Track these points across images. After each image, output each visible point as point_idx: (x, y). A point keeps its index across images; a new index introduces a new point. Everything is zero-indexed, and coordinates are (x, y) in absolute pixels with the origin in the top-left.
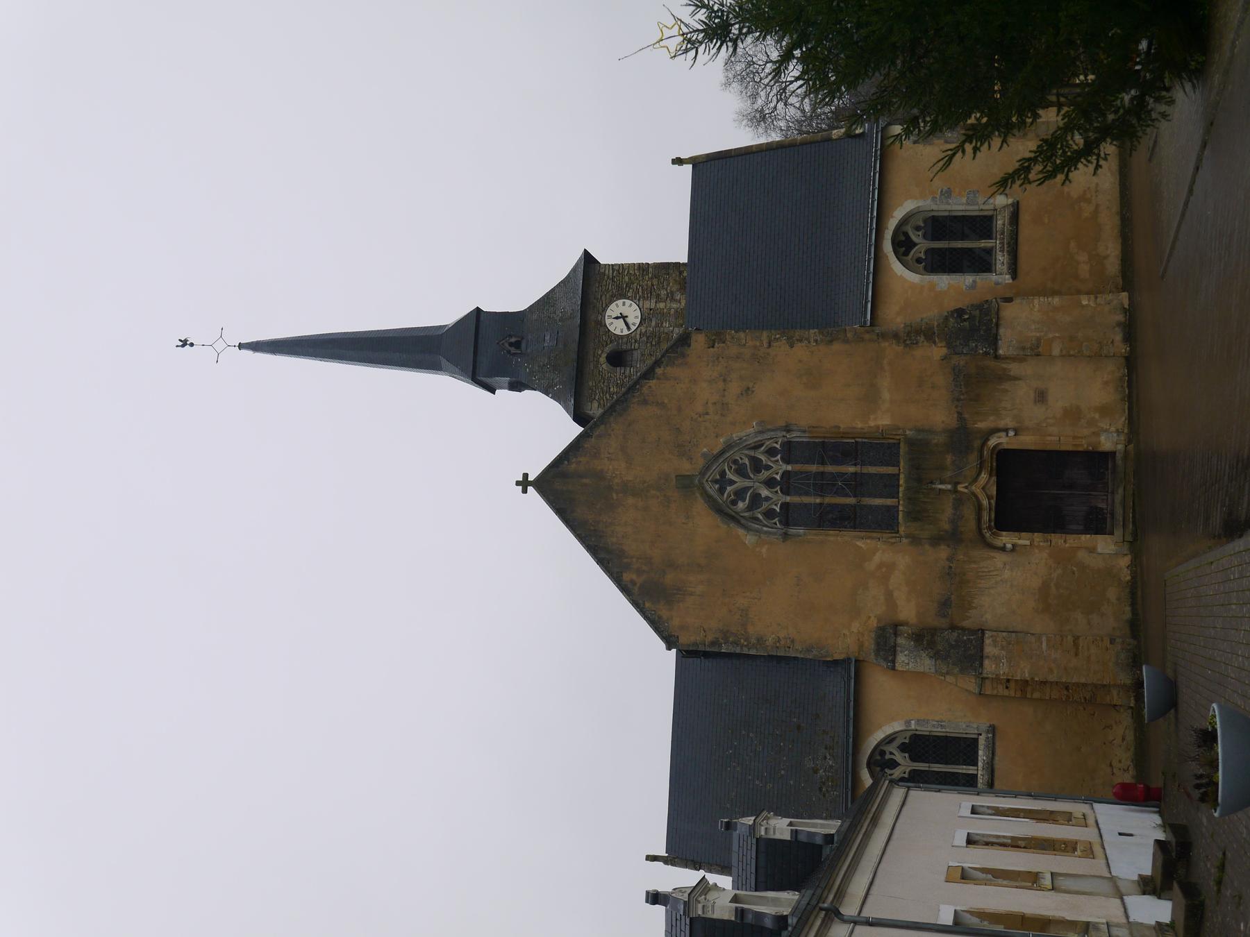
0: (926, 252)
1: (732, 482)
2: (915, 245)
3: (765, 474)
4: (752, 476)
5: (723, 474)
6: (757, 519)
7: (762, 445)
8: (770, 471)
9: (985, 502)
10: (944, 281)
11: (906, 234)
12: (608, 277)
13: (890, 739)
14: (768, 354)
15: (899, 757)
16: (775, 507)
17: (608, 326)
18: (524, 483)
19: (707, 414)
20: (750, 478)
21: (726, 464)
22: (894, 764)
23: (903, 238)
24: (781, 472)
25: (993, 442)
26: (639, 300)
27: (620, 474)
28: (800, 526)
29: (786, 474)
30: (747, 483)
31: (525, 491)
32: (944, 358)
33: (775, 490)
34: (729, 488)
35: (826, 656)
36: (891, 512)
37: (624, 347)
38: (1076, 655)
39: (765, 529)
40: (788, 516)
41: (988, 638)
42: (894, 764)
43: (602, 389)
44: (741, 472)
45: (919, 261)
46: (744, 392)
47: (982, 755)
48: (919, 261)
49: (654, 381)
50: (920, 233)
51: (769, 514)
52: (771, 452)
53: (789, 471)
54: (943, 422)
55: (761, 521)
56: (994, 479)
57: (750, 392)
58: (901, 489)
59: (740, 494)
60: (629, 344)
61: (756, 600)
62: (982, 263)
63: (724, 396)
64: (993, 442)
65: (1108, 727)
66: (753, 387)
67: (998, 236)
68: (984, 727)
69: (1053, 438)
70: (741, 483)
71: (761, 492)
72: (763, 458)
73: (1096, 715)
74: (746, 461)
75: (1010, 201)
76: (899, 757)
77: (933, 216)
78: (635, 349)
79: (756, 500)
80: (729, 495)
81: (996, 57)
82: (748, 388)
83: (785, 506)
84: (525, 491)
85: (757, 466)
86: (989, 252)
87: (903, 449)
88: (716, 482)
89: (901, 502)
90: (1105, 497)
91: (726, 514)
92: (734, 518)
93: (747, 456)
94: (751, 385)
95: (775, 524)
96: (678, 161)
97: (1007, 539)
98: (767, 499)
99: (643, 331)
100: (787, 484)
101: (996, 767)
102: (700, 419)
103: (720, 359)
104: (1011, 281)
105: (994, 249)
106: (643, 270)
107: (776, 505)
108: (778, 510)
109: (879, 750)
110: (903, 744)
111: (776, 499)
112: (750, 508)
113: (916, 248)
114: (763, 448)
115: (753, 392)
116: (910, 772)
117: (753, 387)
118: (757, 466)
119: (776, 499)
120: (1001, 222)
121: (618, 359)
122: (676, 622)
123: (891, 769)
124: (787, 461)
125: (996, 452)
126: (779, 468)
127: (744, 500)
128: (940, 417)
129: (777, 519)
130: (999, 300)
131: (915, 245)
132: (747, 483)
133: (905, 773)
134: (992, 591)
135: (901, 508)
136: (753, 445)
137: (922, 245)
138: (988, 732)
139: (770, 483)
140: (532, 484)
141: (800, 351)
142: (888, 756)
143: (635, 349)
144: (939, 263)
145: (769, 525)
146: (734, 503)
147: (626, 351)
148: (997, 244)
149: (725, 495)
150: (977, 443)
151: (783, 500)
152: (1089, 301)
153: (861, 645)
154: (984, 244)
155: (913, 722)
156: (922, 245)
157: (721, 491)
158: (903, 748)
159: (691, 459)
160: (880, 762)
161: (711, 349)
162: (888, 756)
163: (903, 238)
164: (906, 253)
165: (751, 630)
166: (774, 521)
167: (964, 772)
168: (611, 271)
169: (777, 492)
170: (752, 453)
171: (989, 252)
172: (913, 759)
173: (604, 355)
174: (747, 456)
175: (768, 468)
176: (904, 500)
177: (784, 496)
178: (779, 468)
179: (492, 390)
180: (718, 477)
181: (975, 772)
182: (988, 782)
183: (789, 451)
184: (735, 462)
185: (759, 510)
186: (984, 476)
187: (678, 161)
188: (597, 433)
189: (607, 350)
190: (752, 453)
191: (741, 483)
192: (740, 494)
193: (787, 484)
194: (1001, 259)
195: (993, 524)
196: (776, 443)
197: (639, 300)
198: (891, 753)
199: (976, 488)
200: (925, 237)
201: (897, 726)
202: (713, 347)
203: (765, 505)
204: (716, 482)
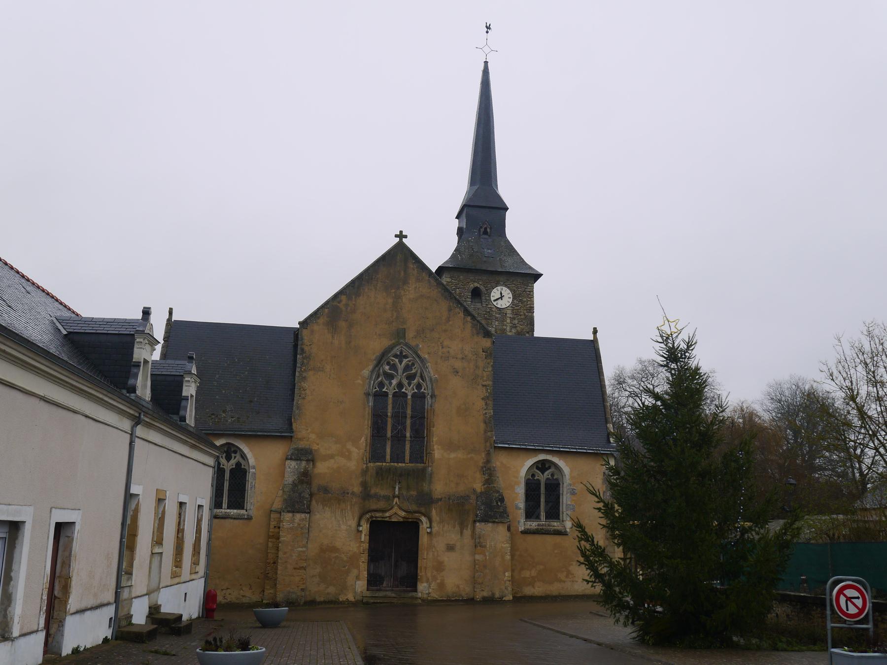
0: (538, 480)
1: (401, 362)
2: (543, 473)
3: (405, 382)
4: (404, 374)
5: (406, 357)
6: (378, 377)
7: (423, 381)
9: (387, 514)
10: (521, 490)
11: (549, 468)
12: (526, 288)
13: (243, 456)
14: (478, 385)
15: (233, 462)
16: (385, 388)
17: (496, 288)
18: (401, 236)
19: (442, 348)
20: (403, 373)
22: (228, 459)
23: (547, 466)
24: (407, 392)
25: (423, 519)
26: (512, 307)
29: (405, 395)
30: (400, 371)
31: (396, 236)
32: (474, 490)
33: (396, 389)
34: (397, 360)
36: (382, 458)
37: (483, 298)
39: (372, 382)
40: (380, 396)
41: (305, 516)
42: (228, 459)
43: (458, 284)
44: (407, 368)
45: (533, 475)
46: (455, 370)
48: (533, 475)
49: (463, 316)
50: (550, 476)
51: (381, 385)
52: (419, 386)
53: (407, 397)
54: (436, 490)
55: (377, 380)
56: (402, 520)
57: (455, 374)
58: (396, 464)
60: (485, 301)
62: (531, 513)
64: (423, 519)
65: (251, 587)
66: (458, 376)
67: (547, 523)
68: (251, 513)
70: (401, 367)
71: (395, 380)
74: (413, 371)
75: (568, 530)
76: (233, 462)
77: (560, 484)
78: (482, 304)
79: (390, 377)
82: (458, 373)
84: (396, 236)
86: (538, 517)
87: (420, 465)
88: (401, 352)
89: (388, 464)
90: (389, 586)
92: (379, 363)
93: (417, 371)
94: (460, 374)
96: (595, 331)
97: (365, 527)
98: (391, 384)
99: (493, 310)
100: (399, 395)
101: (227, 520)
102: (439, 343)
103: (476, 356)
104: (520, 530)
105: (539, 520)
106: (529, 310)
108: (384, 390)
109: (237, 450)
110: (241, 465)
111: (390, 388)
112: (385, 374)
113: (541, 474)
114: (421, 381)
115: (456, 376)
118: (411, 378)
119: (390, 388)
120: (555, 525)
121: (476, 294)
122: (316, 327)
124: (413, 396)
125: (417, 521)
126: (409, 391)
127: (390, 369)
128: (439, 487)
130: (509, 523)
131: (543, 473)
132: (400, 371)
133: (223, 465)
134: (333, 518)
135: (384, 464)
136: (423, 375)
137: (543, 477)
139: (400, 385)
141: (480, 404)
143: (482, 304)
144: (532, 488)
146: (388, 364)
147: (481, 299)
148: (543, 522)
149: (393, 358)
150: (423, 510)
151: (389, 393)
152: (507, 577)
153: (301, 439)
154: (543, 515)
155: (254, 470)
156: (543, 477)
157: (396, 356)
158: (238, 464)
159: (415, 338)
160: (229, 451)
161: (482, 351)
162: (233, 455)
163: (547, 466)
164: (538, 468)
165: (311, 373)
167: (224, 501)
168: (529, 290)
169: (395, 389)
170: (418, 374)
171: (538, 517)
172: (232, 471)
173: (478, 286)
174: (417, 371)
175: (409, 384)
178: (409, 391)
179: (457, 217)
180: (404, 354)
183: (419, 397)
184: (413, 364)
185: (384, 379)
186: (403, 514)
187: (595, 331)
189: (482, 288)
190: (418, 374)
191: (401, 367)
192: (393, 367)
193: (399, 395)
194: (533, 525)
195: (374, 519)
196: (424, 389)
197: (512, 307)
198: (235, 457)
199: (395, 509)
200: (547, 479)
201: (252, 461)
202: (483, 352)
203: (387, 382)
204: (401, 352)
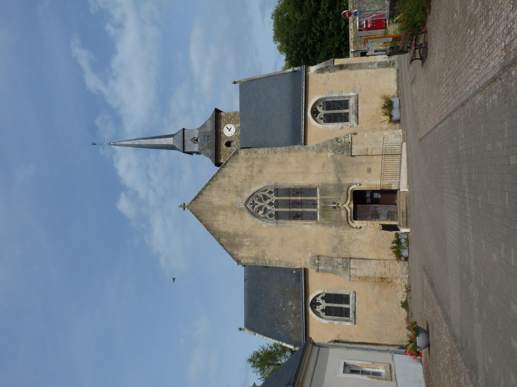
0: (324, 115)
1: (257, 204)
2: (320, 112)
3: (268, 201)
4: (264, 202)
5: (253, 201)
6: (267, 217)
7: (267, 190)
8: (271, 200)
9: (349, 210)
10: (331, 126)
11: (316, 109)
12: (224, 117)
13: (318, 296)
14: (267, 157)
15: (321, 301)
16: (273, 213)
17: (225, 133)
18: (184, 206)
19: (246, 180)
20: (263, 202)
21: (254, 198)
22: (319, 304)
23: (315, 110)
24: (274, 200)
25: (351, 189)
26: (234, 124)
27: (217, 203)
28: (282, 219)
29: (276, 201)
30: (262, 204)
31: (184, 209)
32: (332, 156)
33: (273, 207)
34: (256, 206)
35: (294, 267)
36: (315, 214)
37: (230, 140)
38: (385, 267)
39: (270, 221)
40: (278, 216)
41: (352, 262)
42: (319, 304)
43: (224, 155)
44: (260, 200)
45: (321, 119)
46: (259, 172)
47: (351, 301)
48: (321, 119)
49: (227, 168)
50: (321, 108)
51: (271, 215)
52: (270, 192)
53: (277, 200)
54: (332, 181)
55: (268, 218)
56: (352, 201)
57: (261, 171)
58: (318, 206)
59: (260, 208)
60: (232, 139)
61: (267, 247)
62: (344, 118)
63: (252, 173)
64: (351, 189)
65: (397, 291)
66: (262, 169)
67: (351, 108)
68: (351, 292)
69: (374, 186)
70: (260, 204)
71: (267, 207)
72: (268, 195)
73: (393, 287)
74: (261, 196)
75: (355, 94)
76: (321, 301)
77: (326, 101)
78: (234, 141)
79: (266, 210)
80: (256, 209)
81: (275, 322)
82: (261, 170)
83: (276, 212)
84: (184, 209)
85: (265, 198)
86: (347, 114)
87: (318, 191)
88: (251, 204)
89: (318, 210)
90: (394, 207)
91: (254, 215)
92: (258, 217)
93: (261, 194)
94: (261, 168)
95: (273, 219)
96: (235, 83)
97: (357, 223)
98: (270, 210)
99: (236, 134)
100: (277, 204)
101: (357, 306)
102: (244, 182)
103: (250, 159)
104: (356, 126)
105: (349, 113)
106: (235, 114)
107: (273, 212)
108: (274, 214)
109: (314, 299)
110: (323, 297)
111: (273, 210)
112: (264, 213)
113: (320, 113)
114: (267, 192)
115: (262, 171)
116: (326, 307)
117: (262, 169)
118: (265, 198)
119: (273, 210)
120: (352, 102)
121: (228, 144)
122: (240, 255)
123: (319, 306)
124: (276, 195)
125: (353, 191)
126: (273, 198)
127: (261, 210)
128: (331, 179)
129: (274, 217)
130: (352, 134)
131: (320, 112)
132: (262, 204)
133: (324, 307)
134: (353, 243)
135: (318, 213)
136: (264, 190)
137: (322, 112)
138: (353, 293)
139: (270, 204)
140: (188, 207)
141: (278, 155)
142: (317, 301)
143: (234, 141)
144: (329, 119)
145: (271, 220)
146: (258, 212)
147: (231, 141)
148: (350, 111)
149: (255, 209)
150: (345, 189)
151: (276, 210)
152: (386, 133)
153: (306, 264)
154: (346, 111)
155: (326, 290)
156: (322, 112)
157: (253, 207)
158: (323, 298)
159: (242, 196)
160: (314, 304)
161: (246, 156)
162: (317, 301)
163: (315, 110)
164: (316, 116)
165: (266, 258)
166: (273, 218)
167: (345, 307)
168: (225, 115)
169: (273, 207)
170: (263, 193)
171: (347, 114)
172: (326, 302)
173: (224, 143)
174: (261, 194)
175: (269, 198)
176: (319, 210)
177: (276, 209)
178: (273, 198)
179: (192, 155)
180: (252, 202)
181: (349, 307)
182: (354, 311)
183: (277, 191)
184: (257, 197)
185: (267, 214)
186: (349, 201)
187: (235, 83)
188: (208, 188)
189: (225, 141)
190: (263, 193)
191: (260, 204)
192: (260, 208)
193: (277, 204)
194: (352, 117)
195: (352, 218)
196: (272, 189)
197: (234, 124)
198: (318, 300)
199: (345, 206)
200: (323, 109)
201: (320, 292)
202: (247, 155)
203: (269, 212)
204: (251, 204)
